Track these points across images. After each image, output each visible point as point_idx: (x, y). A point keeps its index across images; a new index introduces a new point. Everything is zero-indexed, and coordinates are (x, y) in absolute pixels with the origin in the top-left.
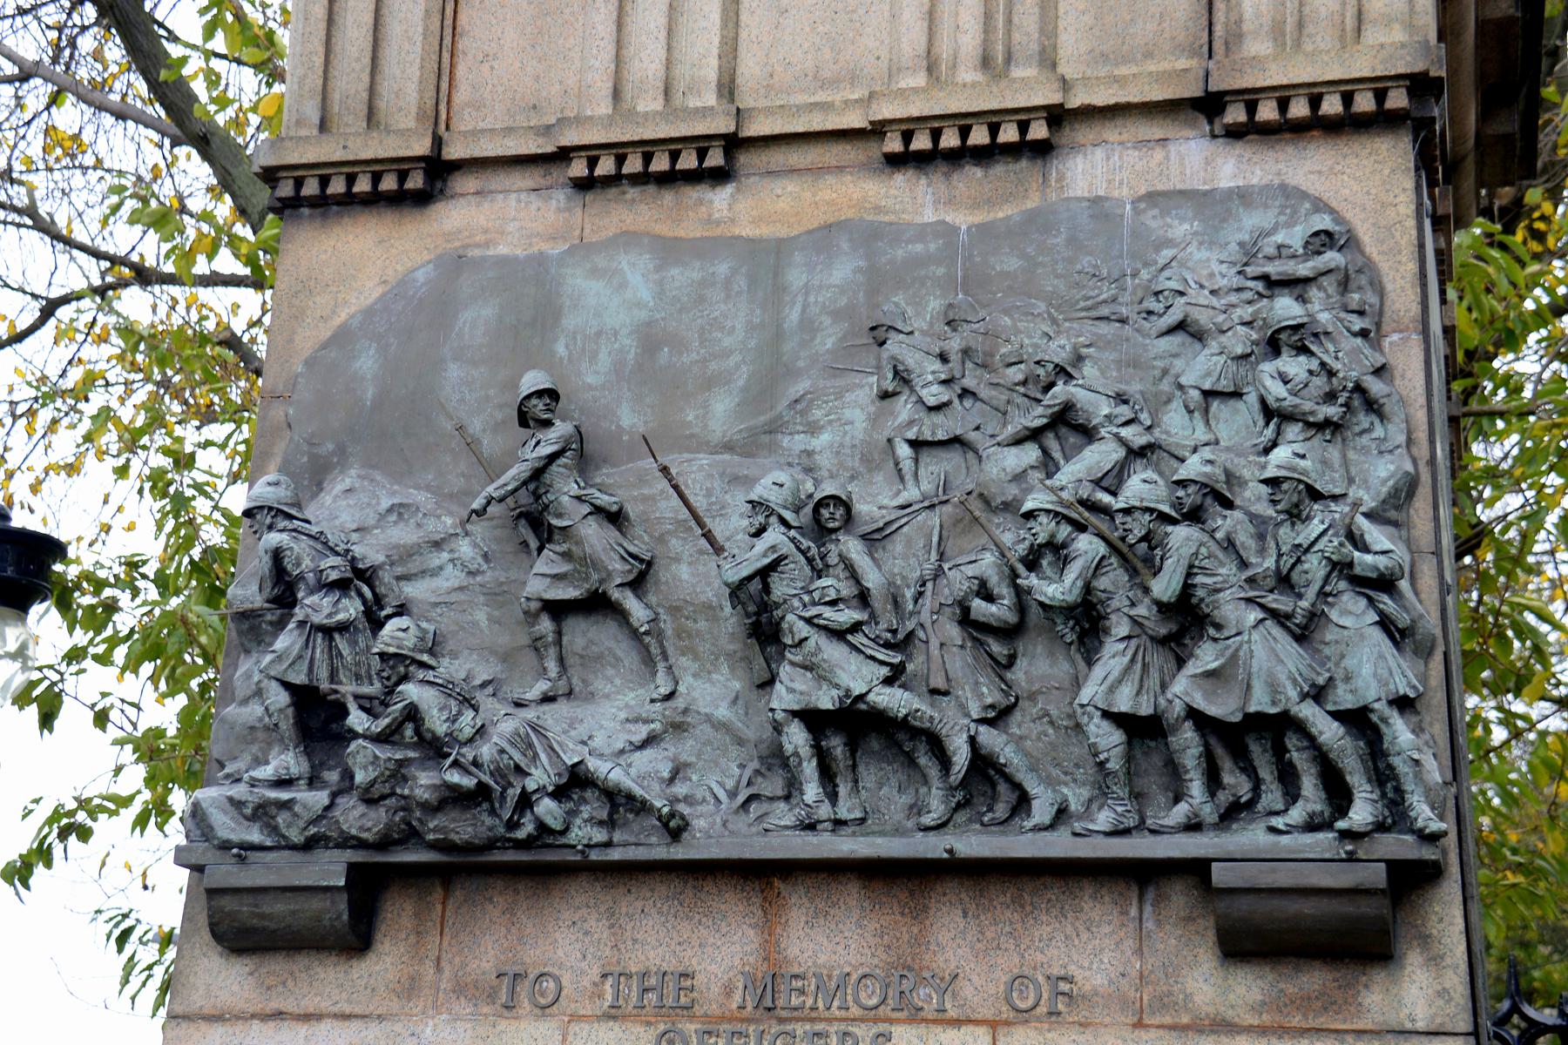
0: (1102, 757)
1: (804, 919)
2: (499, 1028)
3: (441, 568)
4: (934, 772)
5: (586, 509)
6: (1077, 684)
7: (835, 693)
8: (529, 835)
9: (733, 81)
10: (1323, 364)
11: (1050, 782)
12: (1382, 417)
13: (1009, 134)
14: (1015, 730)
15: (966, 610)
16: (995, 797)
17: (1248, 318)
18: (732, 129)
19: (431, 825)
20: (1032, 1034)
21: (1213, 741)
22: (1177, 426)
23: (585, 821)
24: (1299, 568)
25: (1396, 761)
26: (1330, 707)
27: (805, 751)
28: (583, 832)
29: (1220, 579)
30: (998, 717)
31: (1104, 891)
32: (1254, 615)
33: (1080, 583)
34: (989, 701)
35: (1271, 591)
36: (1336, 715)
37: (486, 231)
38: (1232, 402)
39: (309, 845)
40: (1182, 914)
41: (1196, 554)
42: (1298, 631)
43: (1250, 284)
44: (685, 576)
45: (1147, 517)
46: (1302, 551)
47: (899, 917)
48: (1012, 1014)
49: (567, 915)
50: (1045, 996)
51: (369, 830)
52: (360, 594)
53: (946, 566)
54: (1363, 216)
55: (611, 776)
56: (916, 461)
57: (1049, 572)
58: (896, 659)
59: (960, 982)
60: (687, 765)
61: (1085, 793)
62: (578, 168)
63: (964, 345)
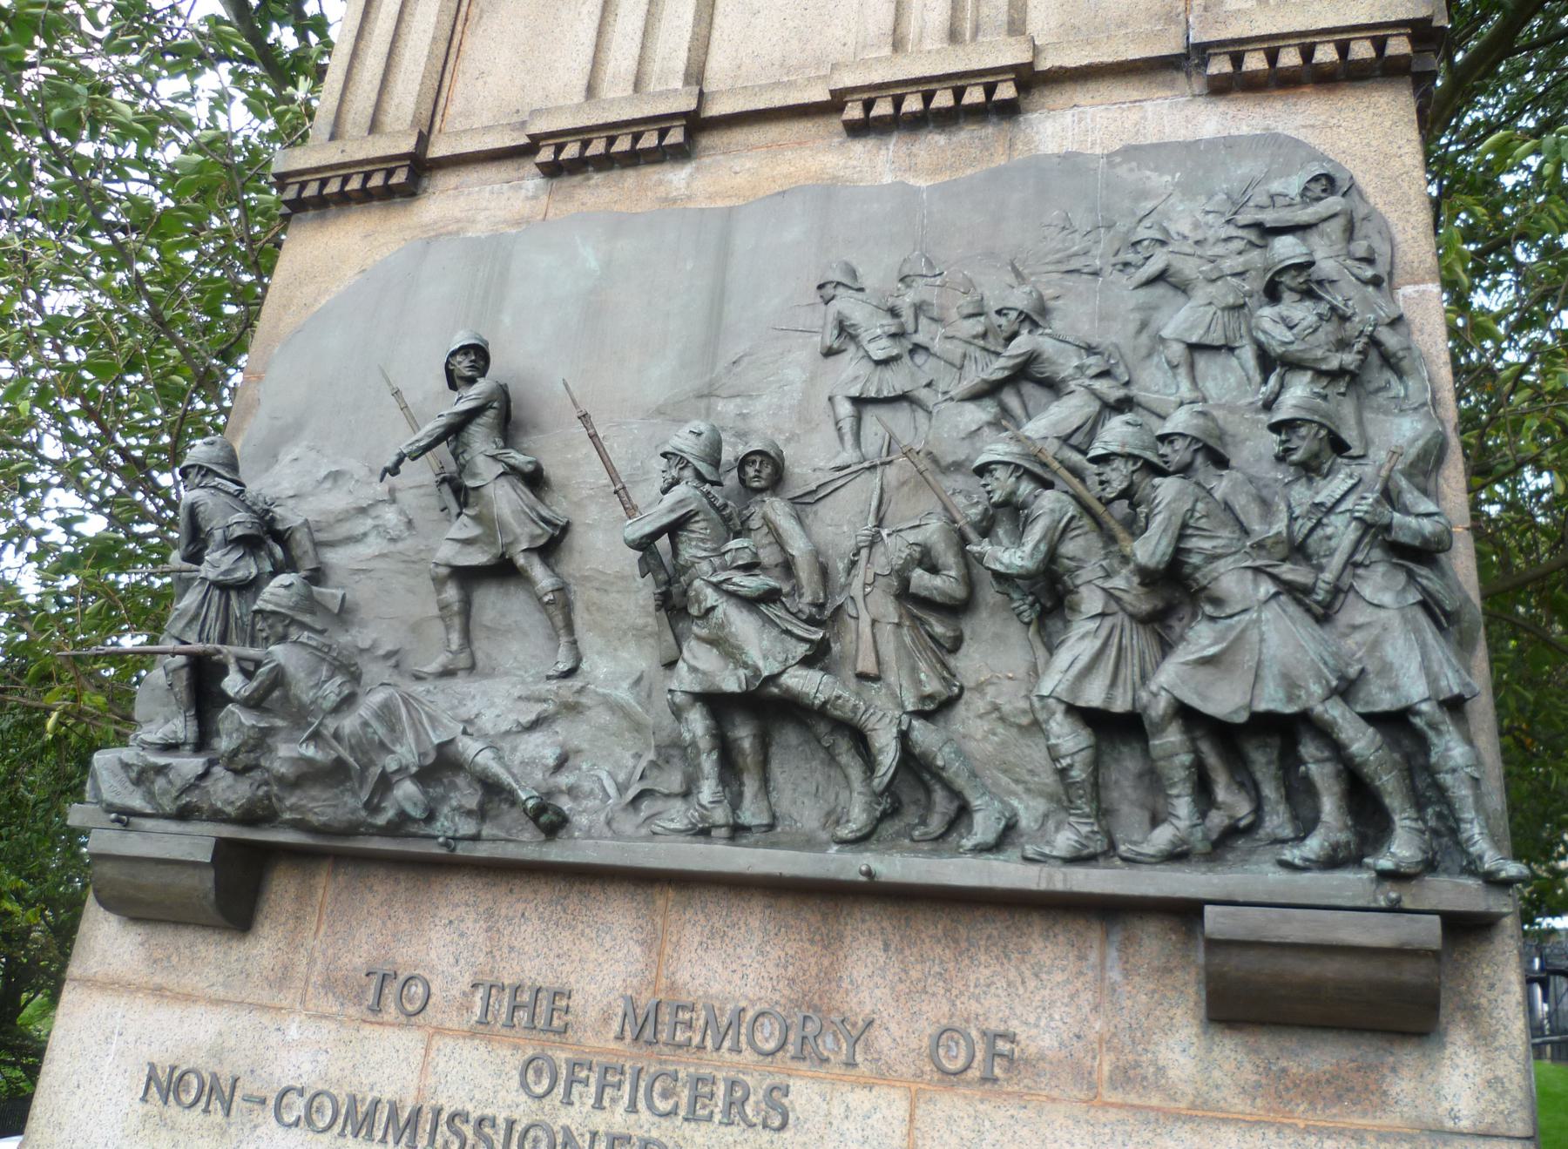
0: (1065, 762)
1: (697, 939)
2: (363, 1033)
3: (365, 535)
4: (856, 772)
5: (500, 469)
6: (1035, 673)
7: (742, 672)
8: (389, 822)
9: (702, 73)
10: (1333, 309)
12: (1400, 374)
13: (975, 96)
15: (905, 582)
16: (929, 807)
17: (1240, 269)
18: (692, 105)
19: (288, 803)
20: (960, 1103)
21: (1205, 746)
22: (1157, 383)
23: (454, 810)
24: (1320, 532)
25: (1447, 779)
26: (1359, 709)
27: (704, 743)
28: (451, 823)
30: (938, 709)
31: (1058, 929)
32: (1266, 588)
33: (1043, 547)
34: (928, 689)
35: (1284, 560)
36: (1371, 718)
37: (458, 221)
38: (1222, 358)
39: (184, 814)
40: (1156, 963)
41: (1193, 510)
42: (1319, 610)
43: (1240, 233)
44: (600, 545)
47: (807, 945)
48: (936, 1076)
49: (445, 913)
50: (979, 1056)
51: (232, 803)
52: (271, 555)
53: (884, 533)
54: (1364, 167)
55: (479, 758)
56: (858, 419)
57: (1005, 541)
58: (818, 635)
59: (875, 1031)
60: (578, 752)
61: (1041, 805)
62: (546, 155)
63: (917, 300)
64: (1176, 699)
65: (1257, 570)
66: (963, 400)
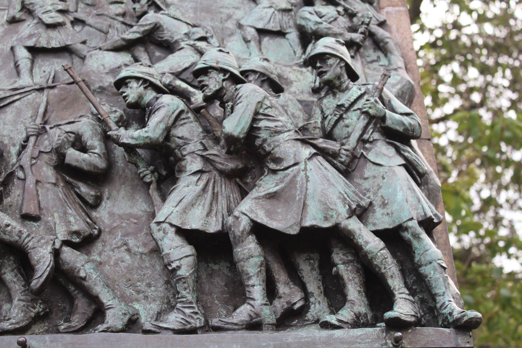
10: (346, 10)
11: (123, 298)
14: (95, 257)
21: (269, 258)
24: (341, 124)
29: (279, 124)
33: (162, 126)
34: (75, 228)
36: (377, 233)
45: (221, 76)
46: (343, 110)
53: (48, 127)
56: (33, 62)
61: (155, 307)
64: (252, 221)
65: (304, 142)
66: (108, 50)
